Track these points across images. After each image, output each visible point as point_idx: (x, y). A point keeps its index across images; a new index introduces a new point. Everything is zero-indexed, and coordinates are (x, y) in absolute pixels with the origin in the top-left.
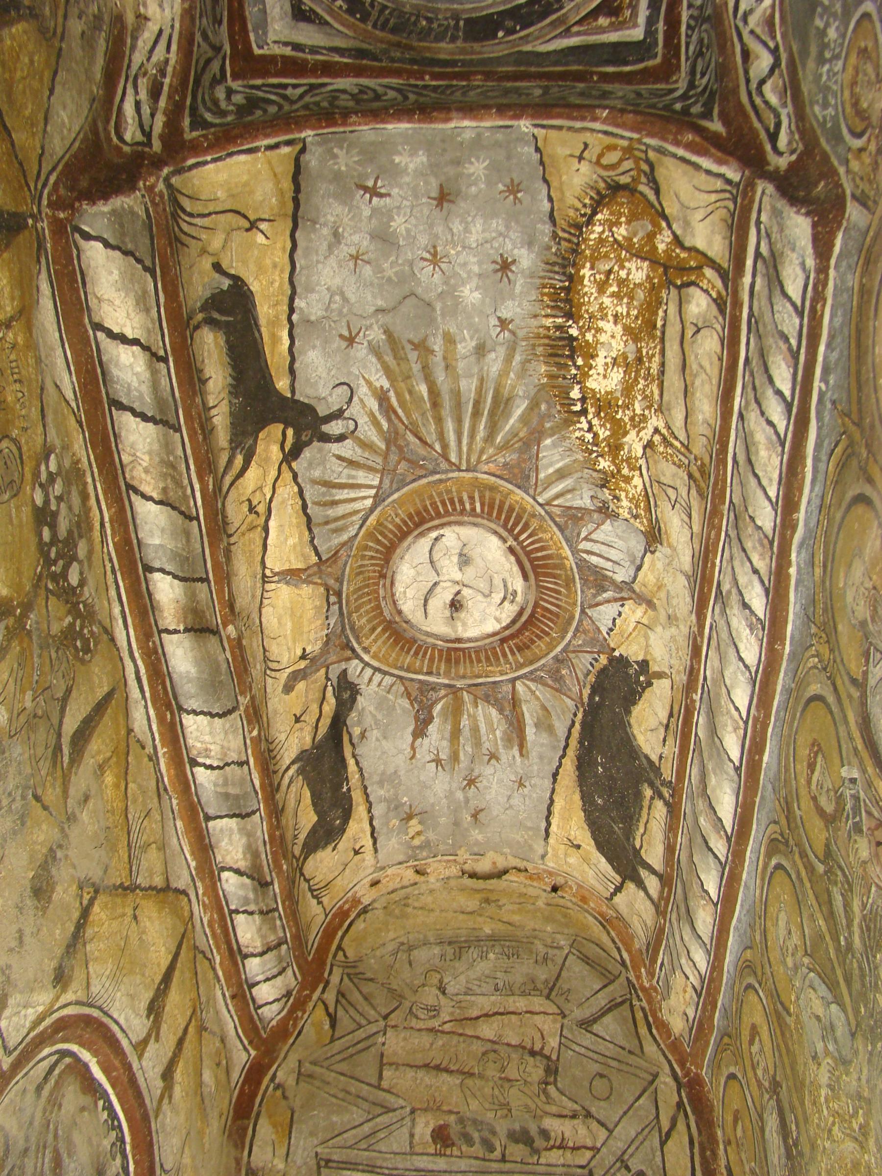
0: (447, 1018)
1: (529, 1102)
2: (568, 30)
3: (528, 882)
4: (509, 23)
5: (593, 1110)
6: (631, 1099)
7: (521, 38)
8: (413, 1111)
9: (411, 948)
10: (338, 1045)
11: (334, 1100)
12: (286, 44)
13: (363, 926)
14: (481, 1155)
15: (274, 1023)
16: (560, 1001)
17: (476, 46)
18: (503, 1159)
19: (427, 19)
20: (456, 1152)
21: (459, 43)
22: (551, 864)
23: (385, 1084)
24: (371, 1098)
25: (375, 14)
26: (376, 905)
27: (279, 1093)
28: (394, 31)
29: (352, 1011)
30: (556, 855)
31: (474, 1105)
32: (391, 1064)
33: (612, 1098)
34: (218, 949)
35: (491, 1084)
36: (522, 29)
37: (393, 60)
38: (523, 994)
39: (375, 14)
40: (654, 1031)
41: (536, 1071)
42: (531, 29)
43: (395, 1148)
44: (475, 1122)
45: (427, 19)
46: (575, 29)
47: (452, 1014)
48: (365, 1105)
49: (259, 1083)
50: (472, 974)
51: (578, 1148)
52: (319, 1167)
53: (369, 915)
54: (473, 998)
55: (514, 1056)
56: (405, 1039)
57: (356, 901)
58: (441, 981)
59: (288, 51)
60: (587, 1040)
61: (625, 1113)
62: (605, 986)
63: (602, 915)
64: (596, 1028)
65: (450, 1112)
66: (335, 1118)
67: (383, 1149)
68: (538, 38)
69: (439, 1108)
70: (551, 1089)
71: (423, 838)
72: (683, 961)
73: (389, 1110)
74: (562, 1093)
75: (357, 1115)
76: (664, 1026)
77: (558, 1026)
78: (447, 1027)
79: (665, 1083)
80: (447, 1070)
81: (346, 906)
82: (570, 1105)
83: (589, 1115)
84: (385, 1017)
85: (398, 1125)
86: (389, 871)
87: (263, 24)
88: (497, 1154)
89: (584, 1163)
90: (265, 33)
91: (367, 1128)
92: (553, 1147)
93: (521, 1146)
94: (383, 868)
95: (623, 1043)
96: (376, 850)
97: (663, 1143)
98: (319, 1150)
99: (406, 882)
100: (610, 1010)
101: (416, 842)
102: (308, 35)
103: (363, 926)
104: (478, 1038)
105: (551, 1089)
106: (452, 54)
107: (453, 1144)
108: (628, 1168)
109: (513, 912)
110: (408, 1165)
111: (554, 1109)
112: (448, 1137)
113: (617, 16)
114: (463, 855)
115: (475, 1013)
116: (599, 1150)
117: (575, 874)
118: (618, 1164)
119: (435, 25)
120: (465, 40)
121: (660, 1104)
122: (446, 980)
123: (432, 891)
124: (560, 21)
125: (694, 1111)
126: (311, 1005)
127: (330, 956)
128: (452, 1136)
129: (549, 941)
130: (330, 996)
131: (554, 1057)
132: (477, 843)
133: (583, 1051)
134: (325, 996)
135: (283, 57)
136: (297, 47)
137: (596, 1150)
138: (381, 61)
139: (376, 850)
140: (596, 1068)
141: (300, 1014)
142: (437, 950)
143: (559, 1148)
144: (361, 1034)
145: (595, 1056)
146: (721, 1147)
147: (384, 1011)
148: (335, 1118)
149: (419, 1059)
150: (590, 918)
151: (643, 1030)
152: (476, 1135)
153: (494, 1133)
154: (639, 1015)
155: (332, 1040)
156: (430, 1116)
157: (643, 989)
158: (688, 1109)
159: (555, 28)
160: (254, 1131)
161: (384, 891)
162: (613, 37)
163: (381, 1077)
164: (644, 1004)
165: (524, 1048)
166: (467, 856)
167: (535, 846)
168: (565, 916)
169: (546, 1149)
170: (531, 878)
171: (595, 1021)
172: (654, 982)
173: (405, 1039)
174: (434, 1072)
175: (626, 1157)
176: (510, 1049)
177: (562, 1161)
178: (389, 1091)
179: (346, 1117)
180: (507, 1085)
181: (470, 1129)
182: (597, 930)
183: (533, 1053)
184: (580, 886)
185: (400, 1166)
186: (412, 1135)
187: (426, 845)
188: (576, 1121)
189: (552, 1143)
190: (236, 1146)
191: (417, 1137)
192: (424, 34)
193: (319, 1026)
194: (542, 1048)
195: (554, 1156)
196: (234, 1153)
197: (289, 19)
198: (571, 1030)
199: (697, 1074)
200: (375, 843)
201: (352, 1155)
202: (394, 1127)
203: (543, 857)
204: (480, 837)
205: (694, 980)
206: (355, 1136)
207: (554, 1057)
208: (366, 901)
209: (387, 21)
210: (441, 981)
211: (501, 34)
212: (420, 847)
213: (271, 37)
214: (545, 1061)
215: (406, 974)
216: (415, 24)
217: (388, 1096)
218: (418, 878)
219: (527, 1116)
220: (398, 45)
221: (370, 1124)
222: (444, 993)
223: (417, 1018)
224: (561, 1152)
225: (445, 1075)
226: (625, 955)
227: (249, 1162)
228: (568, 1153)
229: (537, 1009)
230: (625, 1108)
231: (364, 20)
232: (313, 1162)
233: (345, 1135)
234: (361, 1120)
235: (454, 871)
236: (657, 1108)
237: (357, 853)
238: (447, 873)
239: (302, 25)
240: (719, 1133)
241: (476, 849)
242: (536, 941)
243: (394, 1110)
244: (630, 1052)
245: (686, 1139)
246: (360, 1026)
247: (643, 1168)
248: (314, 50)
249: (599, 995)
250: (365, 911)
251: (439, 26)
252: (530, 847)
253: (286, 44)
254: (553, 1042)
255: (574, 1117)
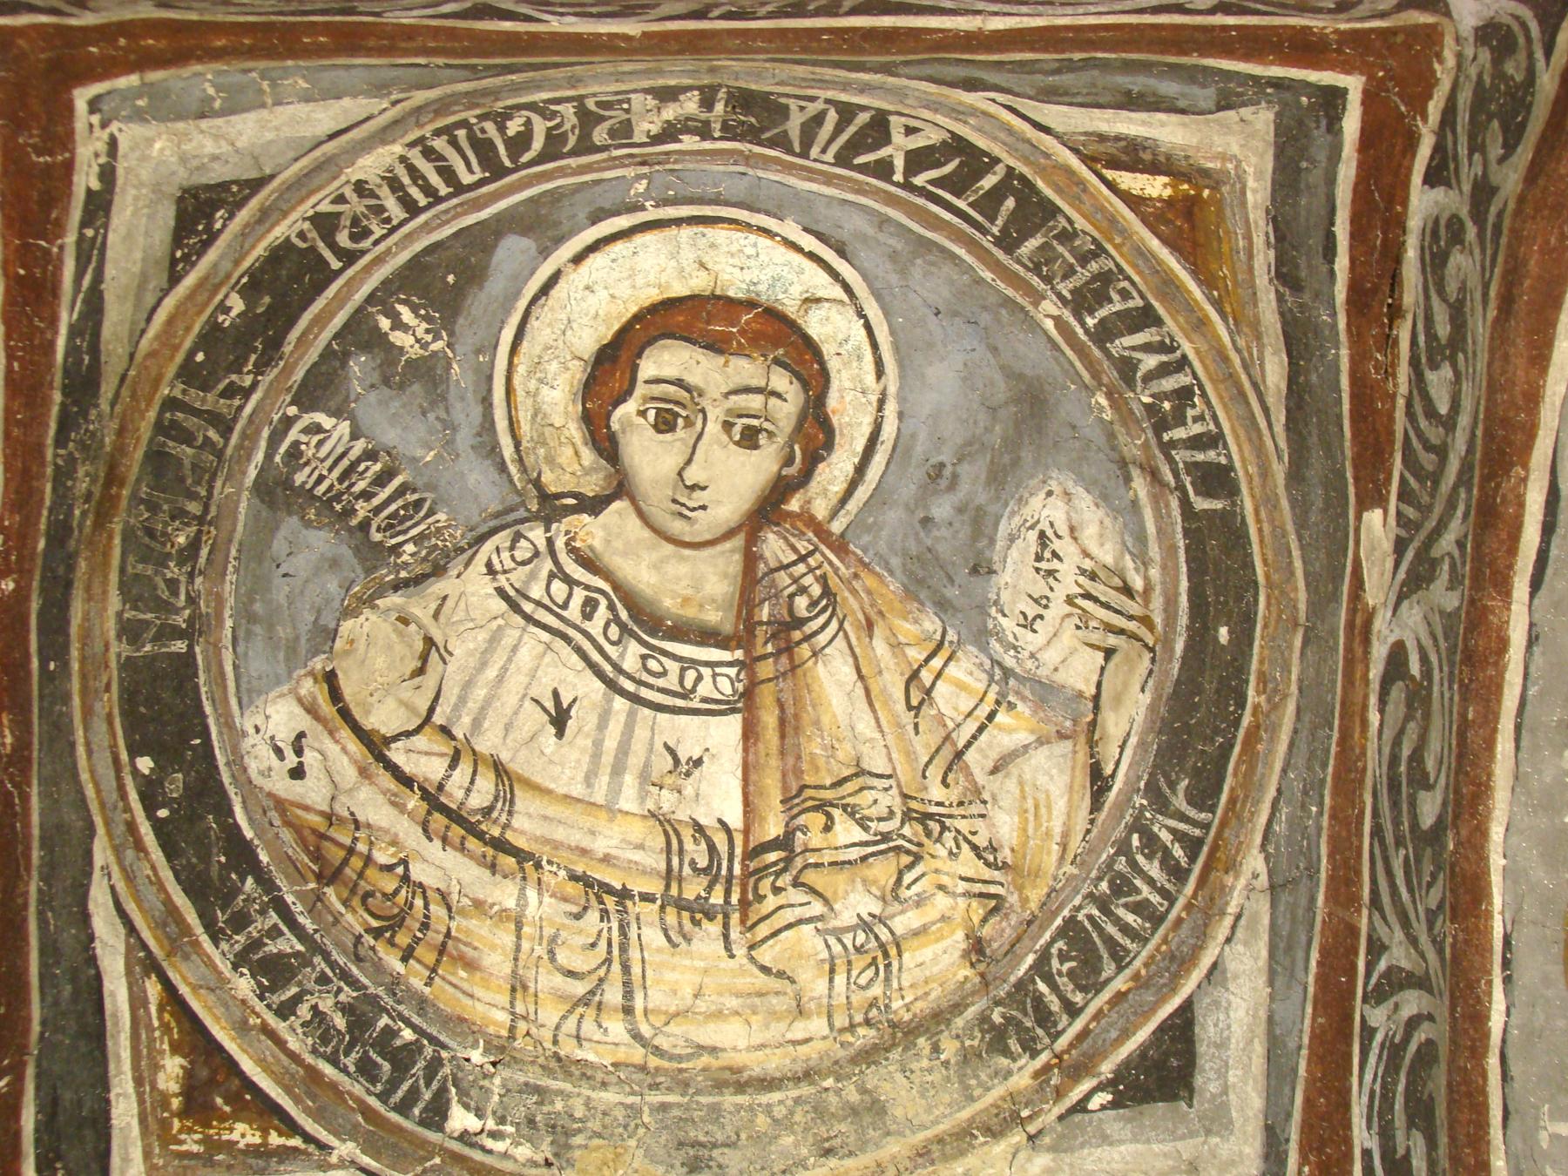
2: (153, 966)
4: (175, 784)
7: (132, 827)
12: (108, 175)
17: (110, 701)
19: (194, 545)
21: (119, 649)
25: (210, 401)
28: (157, 459)
36: (158, 826)
37: (64, 474)
39: (210, 401)
42: (157, 854)
45: (194, 545)
46: (153, 989)
59: (86, 179)
68: (130, 878)
87: (163, 109)
90: (139, 116)
102: (137, 232)
106: (86, 637)
113: (183, 1114)
119: (173, 571)
120: (128, 665)
124: (180, 939)
135: (69, 166)
136: (99, 205)
138: (61, 441)
159: (159, 926)
162: (124, 1111)
192: (146, 545)
197: (183, 177)
209: (187, 438)
211: (145, 764)
213: (128, 134)
216: (178, 514)
220: (113, 478)
231: (188, 373)
239: (167, 215)
248: (91, 253)
251: (172, 585)
253: (108, 175)
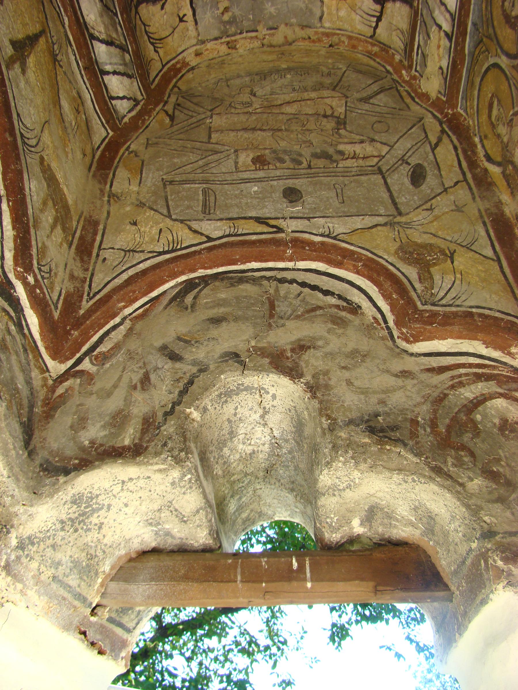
0: (258, 107)
1: (326, 139)
3: (311, 44)
5: (376, 138)
6: (405, 130)
8: (236, 151)
9: (227, 80)
10: (175, 128)
11: (175, 152)
13: (191, 76)
14: (292, 167)
15: (126, 120)
16: (344, 91)
18: (310, 167)
20: (271, 167)
22: (327, 25)
23: (213, 140)
24: (203, 148)
26: (200, 66)
27: (132, 155)
29: (186, 112)
30: (330, 14)
31: (283, 144)
32: (217, 131)
33: (390, 131)
34: (66, 11)
35: (296, 133)
38: (315, 90)
40: (417, 100)
41: (329, 125)
43: (224, 170)
44: (285, 152)
47: (262, 104)
48: (199, 152)
49: (117, 152)
50: (274, 85)
51: (368, 157)
52: (165, 185)
53: (195, 71)
54: (277, 96)
55: (311, 119)
56: (227, 118)
57: (185, 64)
58: (252, 91)
60: (367, 107)
61: (401, 137)
62: (376, 82)
63: (368, 52)
64: (371, 101)
65: (265, 149)
66: (176, 160)
67: (215, 172)
69: (256, 148)
70: (342, 132)
71: (230, 14)
72: (437, 13)
73: (216, 152)
74: (351, 132)
75: (193, 157)
76: (425, 96)
77: (343, 102)
78: (258, 111)
79: (430, 122)
80: (260, 130)
81: (178, 66)
82: (358, 137)
83: (373, 140)
84: (211, 110)
85: (226, 159)
86: (209, 45)
88: (305, 164)
89: (374, 164)
91: (201, 163)
92: (347, 159)
93: (323, 160)
94: (203, 42)
95: (394, 106)
96: (196, 23)
97: (433, 150)
98: (164, 177)
99: (221, 54)
100: (381, 92)
101: (226, 17)
103: (191, 76)
104: (283, 113)
105: (342, 132)
107: (269, 163)
108: (408, 164)
109: (302, 57)
110: (235, 177)
111: (346, 140)
112: (265, 160)
114: (263, 31)
115: (279, 102)
116: (384, 157)
117: (346, 26)
118: (400, 162)
121: (427, 131)
122: (255, 90)
123: (241, 56)
125: (454, 133)
126: (155, 113)
127: (168, 90)
128: (268, 159)
129: (331, 66)
130: (169, 108)
131: (342, 117)
132: (271, 17)
133: (364, 112)
134: (165, 108)
137: (381, 157)
139: (196, 23)
140: (375, 119)
141: (147, 118)
142: (247, 79)
143: (353, 158)
144: (194, 120)
145: (374, 114)
146: (479, 146)
147: (210, 108)
148: (176, 160)
149: (239, 126)
150: (360, 56)
151: (408, 100)
152: (287, 158)
153: (300, 155)
154: (404, 94)
155: (172, 126)
156: (249, 152)
157: (405, 81)
158: (450, 133)
160: (114, 175)
161: (206, 58)
163: (210, 137)
164: (407, 88)
165: (319, 115)
166: (265, 32)
167: (314, 9)
168: (341, 56)
169: (343, 160)
170: (314, 41)
171: (371, 98)
172: (413, 72)
173: (227, 118)
174: (251, 132)
175: (406, 158)
176: (308, 116)
177: (356, 164)
178: (217, 144)
179: (184, 159)
180: (307, 133)
181: (282, 156)
182: (366, 60)
183: (325, 116)
184: (350, 38)
185: (228, 179)
186: (236, 163)
187: (232, 21)
188: (363, 145)
189: (346, 156)
190: (100, 183)
191: (240, 163)
193: (161, 123)
194: (333, 113)
195: (349, 163)
196: (98, 186)
198: (353, 103)
199: (454, 114)
200: (194, 15)
201: (191, 176)
202: (223, 160)
203: (321, 18)
204: (272, 10)
205: (446, 26)
206: (191, 168)
207: (342, 117)
208: (193, 64)
210: (252, 91)
212: (229, 22)
214: (335, 119)
215: (226, 90)
217: (216, 146)
218: (230, 51)
219: (325, 145)
221: (203, 161)
222: (255, 95)
223: (235, 108)
224: (354, 160)
225: (259, 132)
226: (389, 68)
227: (110, 190)
228: (361, 161)
229: (326, 95)
230: (401, 134)
232: (161, 184)
233: (184, 168)
234: (197, 159)
235: (257, 44)
236: (426, 133)
237: (181, 20)
238: (252, 46)
240: (477, 140)
241: (271, 24)
242: (321, 67)
243: (222, 152)
244: (399, 109)
245: (451, 147)
246: (192, 117)
247: (420, 162)
249: (372, 86)
250: (193, 68)
252: (311, 11)
254: (342, 110)
255: (362, 142)
